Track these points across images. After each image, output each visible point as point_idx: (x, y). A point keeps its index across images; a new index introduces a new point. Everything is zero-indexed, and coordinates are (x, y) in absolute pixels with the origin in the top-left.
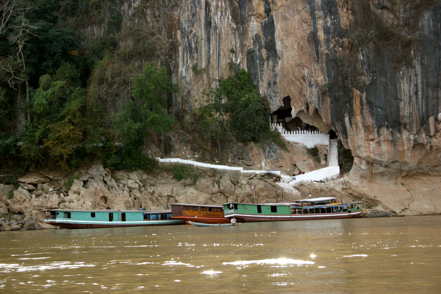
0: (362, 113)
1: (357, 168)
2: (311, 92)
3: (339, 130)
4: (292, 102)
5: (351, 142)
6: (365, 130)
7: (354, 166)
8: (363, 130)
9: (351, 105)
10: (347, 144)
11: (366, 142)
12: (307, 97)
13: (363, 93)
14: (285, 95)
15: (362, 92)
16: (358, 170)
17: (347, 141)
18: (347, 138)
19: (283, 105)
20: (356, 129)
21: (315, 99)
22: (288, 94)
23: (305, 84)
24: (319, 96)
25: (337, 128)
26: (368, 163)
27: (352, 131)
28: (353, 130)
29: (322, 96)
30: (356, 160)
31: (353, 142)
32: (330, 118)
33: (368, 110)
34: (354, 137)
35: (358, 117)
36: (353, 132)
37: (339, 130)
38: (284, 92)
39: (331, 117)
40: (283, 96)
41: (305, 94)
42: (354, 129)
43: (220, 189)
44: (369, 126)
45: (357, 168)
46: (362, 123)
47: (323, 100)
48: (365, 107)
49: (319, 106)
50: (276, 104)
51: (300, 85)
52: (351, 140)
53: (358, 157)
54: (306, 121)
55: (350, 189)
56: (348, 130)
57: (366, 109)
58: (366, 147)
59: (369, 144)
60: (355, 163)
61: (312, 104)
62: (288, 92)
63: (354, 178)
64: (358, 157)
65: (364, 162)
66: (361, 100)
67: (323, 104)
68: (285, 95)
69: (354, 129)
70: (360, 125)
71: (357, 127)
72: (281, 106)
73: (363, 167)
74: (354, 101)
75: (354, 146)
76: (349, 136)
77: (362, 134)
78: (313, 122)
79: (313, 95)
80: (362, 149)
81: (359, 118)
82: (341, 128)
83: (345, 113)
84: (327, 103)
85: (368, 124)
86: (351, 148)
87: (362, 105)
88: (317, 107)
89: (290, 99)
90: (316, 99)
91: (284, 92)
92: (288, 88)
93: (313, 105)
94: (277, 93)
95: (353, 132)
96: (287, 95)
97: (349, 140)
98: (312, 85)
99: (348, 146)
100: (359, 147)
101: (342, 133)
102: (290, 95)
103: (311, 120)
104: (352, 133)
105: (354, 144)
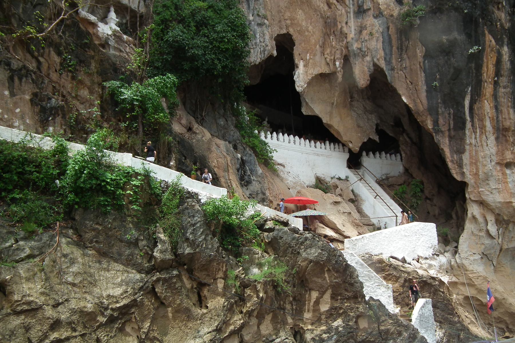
0: (495, 96)
1: (476, 232)
2: (361, 30)
3: (444, 129)
4: (296, 51)
5: (471, 163)
6: (497, 139)
7: (469, 226)
8: (492, 139)
9: (479, 68)
10: (460, 165)
11: (498, 168)
12: (349, 39)
13: (502, 46)
14: (281, 28)
15: (499, 41)
16: (480, 237)
17: (461, 159)
18: (460, 151)
19: (275, 53)
20: (482, 133)
21: (376, 45)
22: (287, 27)
23: (339, 7)
24: (389, 36)
25: (441, 121)
26: (499, 221)
27: (473, 136)
28: (475, 132)
29: (400, 39)
30: (474, 210)
31: (475, 162)
32: (423, 95)
33: (508, 89)
34: (476, 151)
35: (486, 102)
36: (476, 138)
37: (444, 129)
38: (280, 21)
39: (427, 91)
40: (277, 31)
41: (345, 30)
42: (478, 131)
43: (180, 251)
44: (507, 130)
45: (476, 232)
46: (492, 119)
47: (400, 48)
48: (504, 81)
49: (388, 62)
50: (261, 47)
51: (326, 8)
52: (471, 157)
53: (482, 203)
54: (316, 106)
55: (471, 285)
56: (467, 132)
57: (505, 87)
58: (498, 181)
59: (504, 174)
60: (474, 217)
61: (364, 56)
62: (288, 22)
63: (472, 258)
64: (482, 203)
65: (491, 218)
66: (499, 63)
67: (402, 59)
68: (281, 28)
69: (478, 131)
70: (488, 124)
71: (483, 127)
72: (271, 56)
73: (493, 229)
74: (485, 60)
75: (476, 174)
76: (467, 147)
77: (489, 147)
78: (331, 114)
79: (371, 34)
80: (493, 184)
81: (487, 106)
82: (452, 123)
83: (468, 85)
84: (415, 56)
85: (507, 124)
86: (469, 179)
87: (498, 73)
88: (382, 64)
89: (292, 43)
90: (380, 45)
91: (280, 21)
92: (288, 14)
93: (368, 58)
94: (265, 17)
95: (476, 138)
96: (284, 31)
97: (466, 158)
98: (365, 11)
99: (463, 174)
100: (487, 178)
101: (451, 138)
102: (291, 31)
103: (329, 109)
104: (473, 141)
105: (477, 169)
